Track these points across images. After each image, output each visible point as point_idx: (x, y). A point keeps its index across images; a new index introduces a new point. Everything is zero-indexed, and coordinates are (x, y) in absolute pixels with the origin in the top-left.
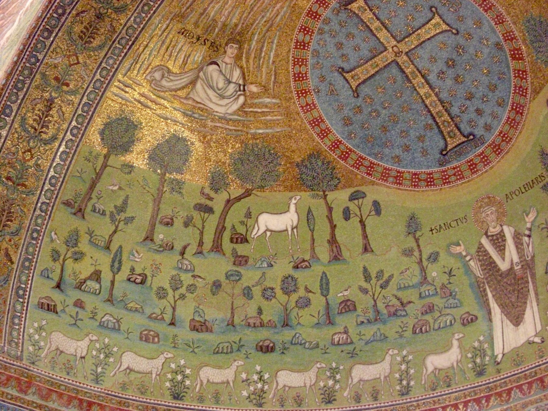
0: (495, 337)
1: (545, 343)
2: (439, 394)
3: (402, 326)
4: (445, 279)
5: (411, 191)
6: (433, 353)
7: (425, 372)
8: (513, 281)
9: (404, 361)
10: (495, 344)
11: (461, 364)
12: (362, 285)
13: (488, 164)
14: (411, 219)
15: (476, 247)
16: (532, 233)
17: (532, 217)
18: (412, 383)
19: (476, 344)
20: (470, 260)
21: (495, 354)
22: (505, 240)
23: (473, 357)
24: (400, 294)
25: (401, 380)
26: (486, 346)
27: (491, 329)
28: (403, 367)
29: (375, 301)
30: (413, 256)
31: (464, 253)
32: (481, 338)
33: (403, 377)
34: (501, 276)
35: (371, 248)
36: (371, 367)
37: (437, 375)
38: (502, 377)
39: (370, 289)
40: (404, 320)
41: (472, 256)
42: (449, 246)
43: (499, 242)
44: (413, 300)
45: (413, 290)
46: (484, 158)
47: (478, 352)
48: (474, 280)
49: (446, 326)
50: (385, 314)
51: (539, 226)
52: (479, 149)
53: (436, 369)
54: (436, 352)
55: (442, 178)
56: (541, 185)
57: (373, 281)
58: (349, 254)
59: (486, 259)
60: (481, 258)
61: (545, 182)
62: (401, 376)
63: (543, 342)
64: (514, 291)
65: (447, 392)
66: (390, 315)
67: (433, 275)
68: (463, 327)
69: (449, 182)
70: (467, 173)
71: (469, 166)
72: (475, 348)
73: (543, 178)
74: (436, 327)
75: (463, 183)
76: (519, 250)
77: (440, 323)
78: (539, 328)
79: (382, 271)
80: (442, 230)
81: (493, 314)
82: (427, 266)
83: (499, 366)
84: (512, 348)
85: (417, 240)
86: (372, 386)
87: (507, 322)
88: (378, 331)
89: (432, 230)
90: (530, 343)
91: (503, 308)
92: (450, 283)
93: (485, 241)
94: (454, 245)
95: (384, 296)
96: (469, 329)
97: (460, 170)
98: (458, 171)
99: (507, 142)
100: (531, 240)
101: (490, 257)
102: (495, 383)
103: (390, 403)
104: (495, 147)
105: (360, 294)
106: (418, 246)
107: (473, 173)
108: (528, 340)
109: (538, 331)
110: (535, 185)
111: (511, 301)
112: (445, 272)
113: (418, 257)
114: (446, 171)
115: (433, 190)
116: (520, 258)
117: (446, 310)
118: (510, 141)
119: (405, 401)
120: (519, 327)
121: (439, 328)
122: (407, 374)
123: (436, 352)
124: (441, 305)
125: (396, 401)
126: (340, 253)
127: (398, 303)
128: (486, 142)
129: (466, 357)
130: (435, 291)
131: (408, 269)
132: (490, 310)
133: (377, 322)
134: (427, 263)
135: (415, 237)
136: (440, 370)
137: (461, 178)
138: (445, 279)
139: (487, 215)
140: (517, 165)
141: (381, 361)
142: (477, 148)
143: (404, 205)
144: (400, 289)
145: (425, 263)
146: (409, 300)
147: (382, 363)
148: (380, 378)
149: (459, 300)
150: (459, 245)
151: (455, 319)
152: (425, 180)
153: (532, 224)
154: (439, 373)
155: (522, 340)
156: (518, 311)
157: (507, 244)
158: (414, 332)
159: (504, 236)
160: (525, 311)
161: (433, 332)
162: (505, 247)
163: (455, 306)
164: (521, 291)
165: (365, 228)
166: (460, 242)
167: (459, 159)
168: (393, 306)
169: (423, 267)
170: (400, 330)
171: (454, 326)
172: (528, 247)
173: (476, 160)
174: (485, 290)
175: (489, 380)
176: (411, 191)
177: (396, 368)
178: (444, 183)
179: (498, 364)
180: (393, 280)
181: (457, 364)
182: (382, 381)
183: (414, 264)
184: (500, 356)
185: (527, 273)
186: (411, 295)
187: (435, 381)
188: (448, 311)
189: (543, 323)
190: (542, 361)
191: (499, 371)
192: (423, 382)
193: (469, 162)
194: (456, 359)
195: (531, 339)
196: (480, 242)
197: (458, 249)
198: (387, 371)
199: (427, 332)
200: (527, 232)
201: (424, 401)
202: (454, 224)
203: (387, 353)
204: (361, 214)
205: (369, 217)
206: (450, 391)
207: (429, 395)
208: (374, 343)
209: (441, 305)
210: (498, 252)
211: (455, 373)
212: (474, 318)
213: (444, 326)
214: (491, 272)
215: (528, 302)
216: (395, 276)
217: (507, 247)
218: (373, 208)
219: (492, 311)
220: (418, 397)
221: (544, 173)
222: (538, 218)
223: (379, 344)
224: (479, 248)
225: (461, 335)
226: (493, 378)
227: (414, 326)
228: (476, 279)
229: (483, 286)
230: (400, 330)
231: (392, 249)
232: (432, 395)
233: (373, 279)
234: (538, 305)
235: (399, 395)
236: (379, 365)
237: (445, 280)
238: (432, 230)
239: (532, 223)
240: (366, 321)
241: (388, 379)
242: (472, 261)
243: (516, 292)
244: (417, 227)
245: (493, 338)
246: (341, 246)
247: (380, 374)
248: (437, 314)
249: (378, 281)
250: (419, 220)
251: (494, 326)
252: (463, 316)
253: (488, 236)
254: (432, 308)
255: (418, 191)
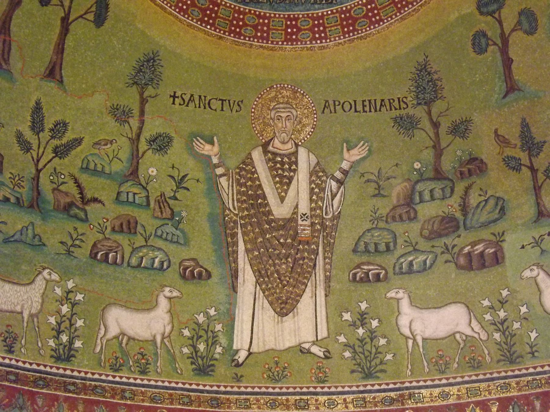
0: (237, 319)
1: (329, 360)
2: (124, 380)
3: (75, 236)
4: (169, 187)
5: (171, 14)
6: (122, 306)
7: (102, 332)
8: (289, 241)
9: (67, 299)
10: (235, 332)
11: (170, 341)
12: (24, 133)
13: (320, 38)
14: (148, 61)
15: (240, 160)
16: (347, 179)
17: (356, 154)
18: (78, 344)
19: (201, 318)
20: (221, 176)
21: (235, 347)
22: (295, 171)
23: (192, 338)
24: (84, 178)
25: (59, 332)
26: (219, 327)
27: (232, 304)
28: (65, 309)
29: (39, 171)
30: (126, 125)
31: (215, 160)
32: (212, 312)
33: (62, 328)
34: (269, 223)
35: (62, 77)
36: (7, 286)
37: (124, 345)
38: (242, 389)
39: (35, 147)
40: (82, 227)
41: (227, 170)
42: (194, 135)
43: (283, 170)
44: (103, 198)
45: (108, 182)
46: (318, 26)
47: (202, 333)
48: (218, 211)
49: (152, 268)
50: (49, 202)
51: (363, 175)
52: (319, 9)
53: (123, 334)
54: (128, 305)
55: (231, 21)
56: (395, 113)
57: (45, 135)
58: (20, 65)
59: (251, 186)
60: (243, 181)
61: (403, 112)
62: (59, 324)
63: (327, 358)
64: (287, 257)
65: (138, 381)
66: (57, 209)
67: (151, 170)
68: (182, 281)
69: (239, 34)
70: (279, 36)
71: (287, 27)
72: (197, 324)
73: (403, 105)
74: (134, 261)
75: (261, 47)
76: (315, 197)
77: (142, 258)
78: (323, 333)
79: (65, 125)
80: (191, 105)
81: (240, 279)
82: (144, 153)
83: (238, 369)
84: (267, 348)
85: (143, 102)
86: (7, 322)
87: (263, 302)
88: (30, 228)
89: (174, 97)
90: (301, 351)
91: (261, 276)
92: (176, 199)
93: (257, 155)
94: (202, 139)
95: (55, 169)
96: (190, 287)
97: (268, 25)
98: (264, 24)
99: (371, 21)
100: (342, 188)
101: (260, 186)
102: (228, 396)
103: (34, 367)
104: (346, 19)
105: (16, 148)
106: (142, 113)
107: (287, 40)
108: (300, 345)
109: (319, 338)
110: (383, 109)
111: (277, 272)
112: (172, 177)
113: (135, 129)
114: (245, 14)
115: (206, 33)
116: (312, 209)
117: (157, 239)
118: (378, 22)
119: (61, 371)
120: (285, 318)
121: (139, 266)
122: (71, 325)
123: (128, 305)
124: (150, 229)
125: (45, 366)
126: (6, 56)
127: (74, 191)
128: (337, 4)
129: (181, 334)
130: (144, 199)
131: (111, 142)
132: (236, 271)
133: (30, 210)
134: (146, 148)
135: (141, 94)
136: (130, 338)
137: (262, 38)
138: (169, 187)
139: (279, 118)
140: (368, 64)
141: (28, 284)
142: (316, 6)
143: (147, 31)
144: (85, 169)
145: (143, 146)
146: (96, 196)
147: (28, 288)
148: (21, 313)
149: (182, 231)
150: (212, 143)
151: (170, 262)
152: (203, 11)
153: (351, 167)
154: (127, 344)
155: (289, 342)
156: (288, 292)
157: (295, 178)
158: (93, 256)
159: (296, 163)
160: (301, 296)
161: (128, 271)
162: (290, 182)
163: (175, 239)
164: (301, 262)
165: (66, 35)
166: (215, 139)
167: (276, 6)
168: (66, 194)
169: (138, 150)
170: (70, 243)
171: (165, 273)
172: (332, 200)
173: (304, 23)
174: (234, 235)
175: (219, 386)
176: (171, 14)
177: (54, 306)
178: (230, 32)
179: (238, 365)
180: (79, 149)
181: (163, 338)
182: (26, 320)
183: (124, 139)
184: (242, 356)
185: (318, 237)
186: (103, 188)
187: (119, 355)
188: (160, 243)
189: (332, 327)
190: (322, 388)
191: (238, 379)
192: (98, 349)
193: (291, 20)
194: (162, 330)
195: (306, 346)
196: (250, 154)
197: (207, 149)
198: (34, 305)
199: (115, 263)
200: (338, 175)
201: (97, 384)
202: (216, 105)
203: (40, 273)
204: (70, 8)
205: (80, 20)
206: (146, 382)
207: (107, 376)
208: (20, 246)
209: (150, 229)
210: (275, 183)
211: (156, 354)
212: (204, 273)
213: (150, 267)
214: (252, 211)
215: (309, 284)
216: (83, 144)
217: (294, 182)
218: (94, 9)
219: (240, 274)
220: (86, 373)
221: (410, 99)
222: (367, 163)
223: (29, 252)
224: (244, 163)
225: (175, 294)
226: (225, 387)
227: (95, 245)
228: (224, 211)
229: (233, 229)
230: (70, 243)
231: (97, 95)
232: (110, 378)
233: (47, 130)
234: (326, 296)
235: (52, 356)
236: (23, 288)
237: (169, 189)
238: (174, 97)
239: (354, 165)
240: (13, 200)
241: (35, 320)
242: (225, 178)
243: (289, 260)
244: (152, 79)
245: (233, 320)
246: (14, 44)
247: (23, 307)
248: (139, 241)
249: (52, 137)
250: (161, 69)
251: (239, 300)
252: (187, 264)
253: (266, 152)
254: (132, 225)
255: (180, 21)
